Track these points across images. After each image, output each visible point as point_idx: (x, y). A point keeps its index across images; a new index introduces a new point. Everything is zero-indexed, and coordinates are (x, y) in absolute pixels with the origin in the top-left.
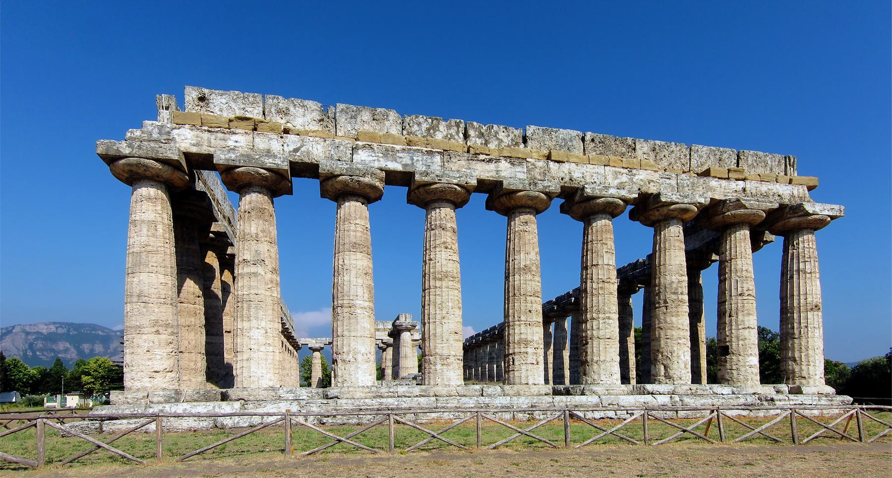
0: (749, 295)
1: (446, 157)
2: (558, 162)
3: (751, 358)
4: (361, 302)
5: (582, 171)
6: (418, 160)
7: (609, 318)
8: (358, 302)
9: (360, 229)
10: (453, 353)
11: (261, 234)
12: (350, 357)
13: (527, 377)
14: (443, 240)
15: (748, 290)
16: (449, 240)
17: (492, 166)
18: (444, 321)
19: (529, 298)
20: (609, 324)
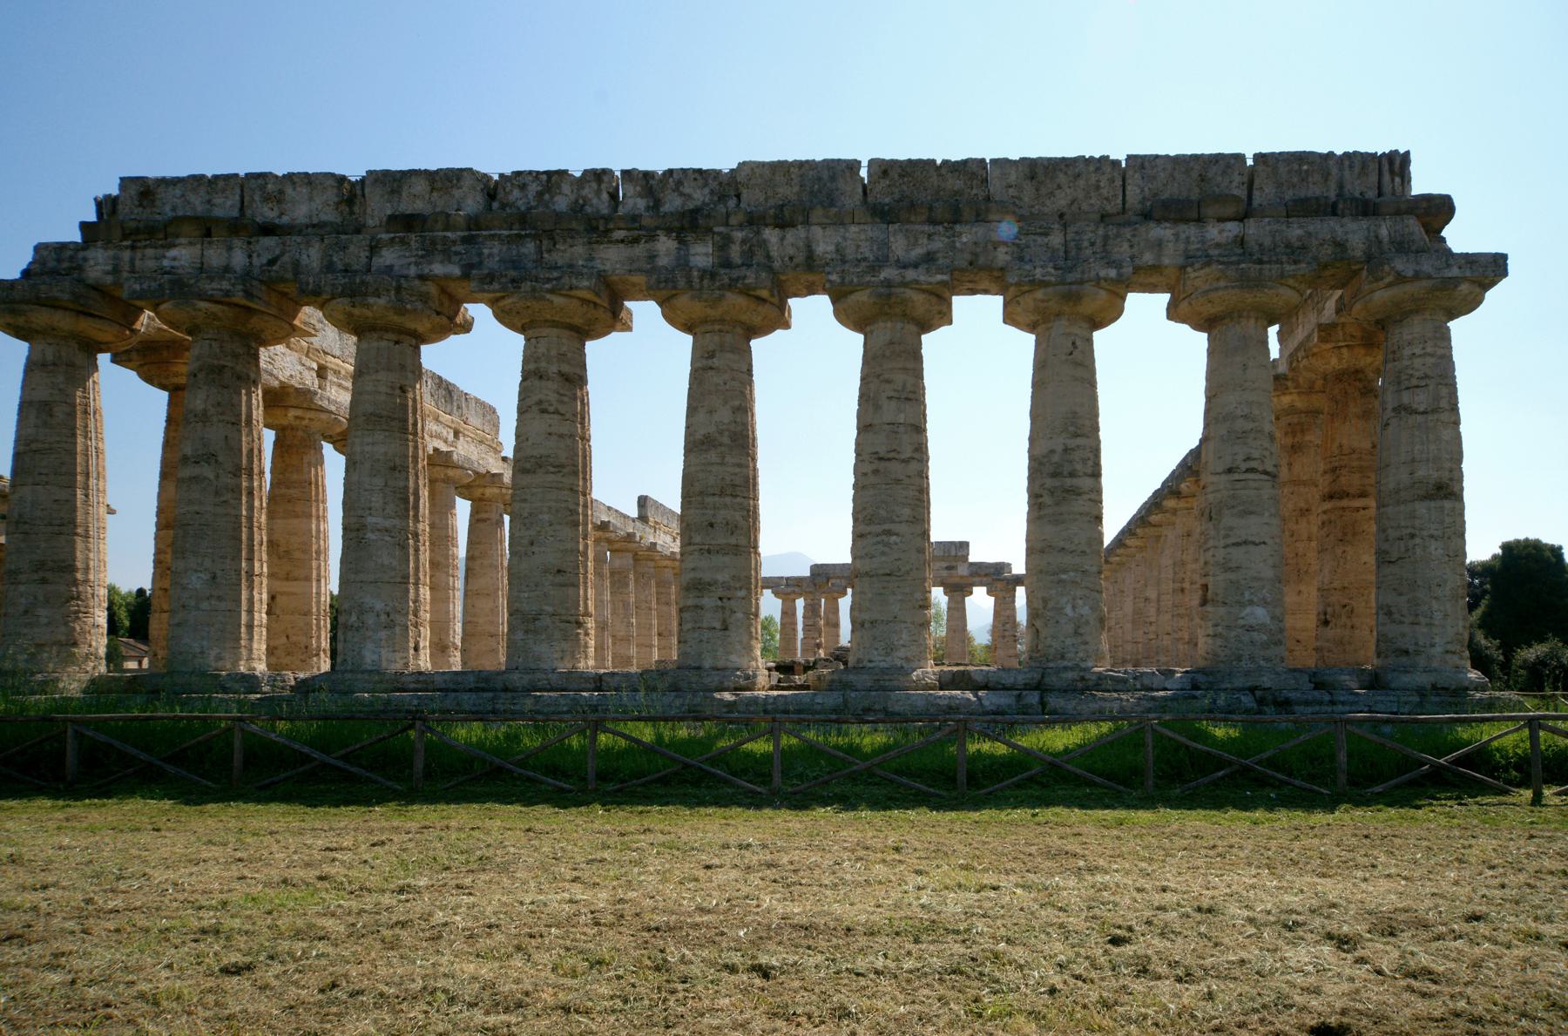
0: (1247, 471)
1: (545, 242)
3: (1248, 610)
4: (380, 520)
6: (490, 255)
7: (889, 533)
8: (374, 520)
9: (383, 389)
10: (549, 609)
11: (212, 411)
12: (354, 618)
13: (700, 654)
14: (535, 398)
15: (1248, 459)
16: (553, 397)
18: (535, 549)
19: (709, 500)
20: (887, 545)
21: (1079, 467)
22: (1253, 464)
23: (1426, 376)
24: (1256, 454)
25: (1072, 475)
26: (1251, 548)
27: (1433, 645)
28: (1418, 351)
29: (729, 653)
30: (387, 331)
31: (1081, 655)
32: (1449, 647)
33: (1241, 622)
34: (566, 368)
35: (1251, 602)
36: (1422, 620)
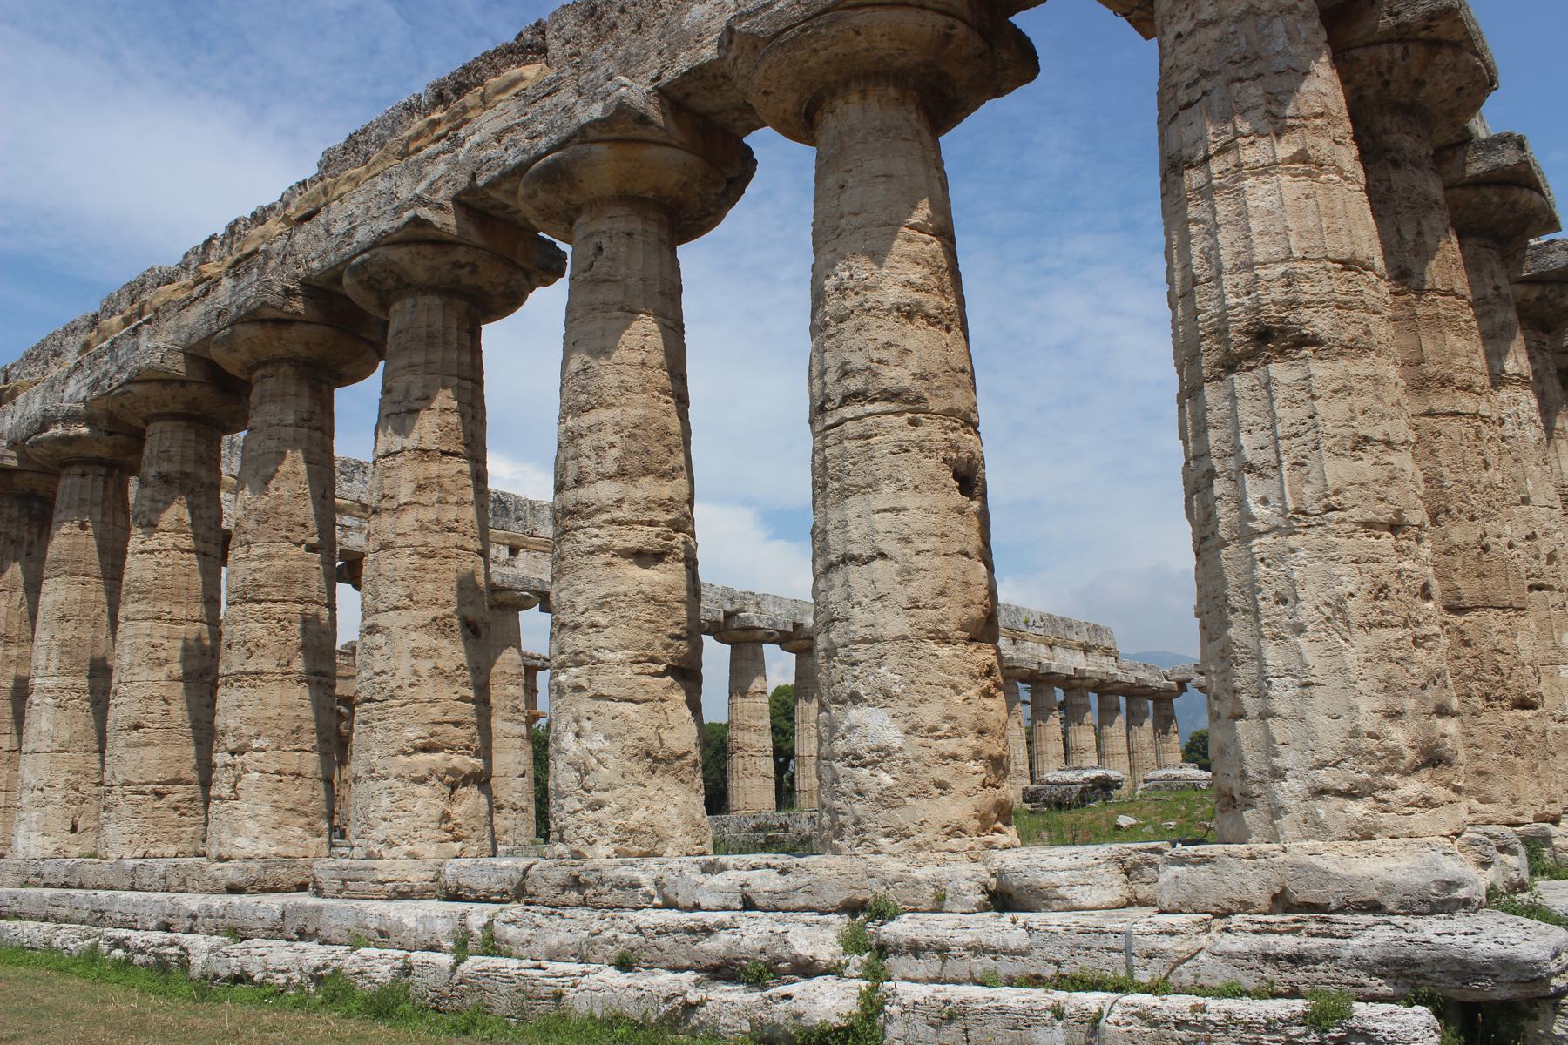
2: (308, 217)
3: (855, 714)
5: (351, 207)
10: (120, 778)
15: (845, 373)
17: (209, 299)
21: (589, 465)
22: (854, 384)
23: (1205, 74)
24: (857, 361)
25: (579, 482)
26: (855, 573)
27: (1278, 774)
28: (1184, 26)
29: (236, 834)
30: (71, 464)
31: (586, 831)
32: (1326, 777)
33: (840, 746)
34: (165, 467)
35: (856, 698)
36: (1249, 703)
